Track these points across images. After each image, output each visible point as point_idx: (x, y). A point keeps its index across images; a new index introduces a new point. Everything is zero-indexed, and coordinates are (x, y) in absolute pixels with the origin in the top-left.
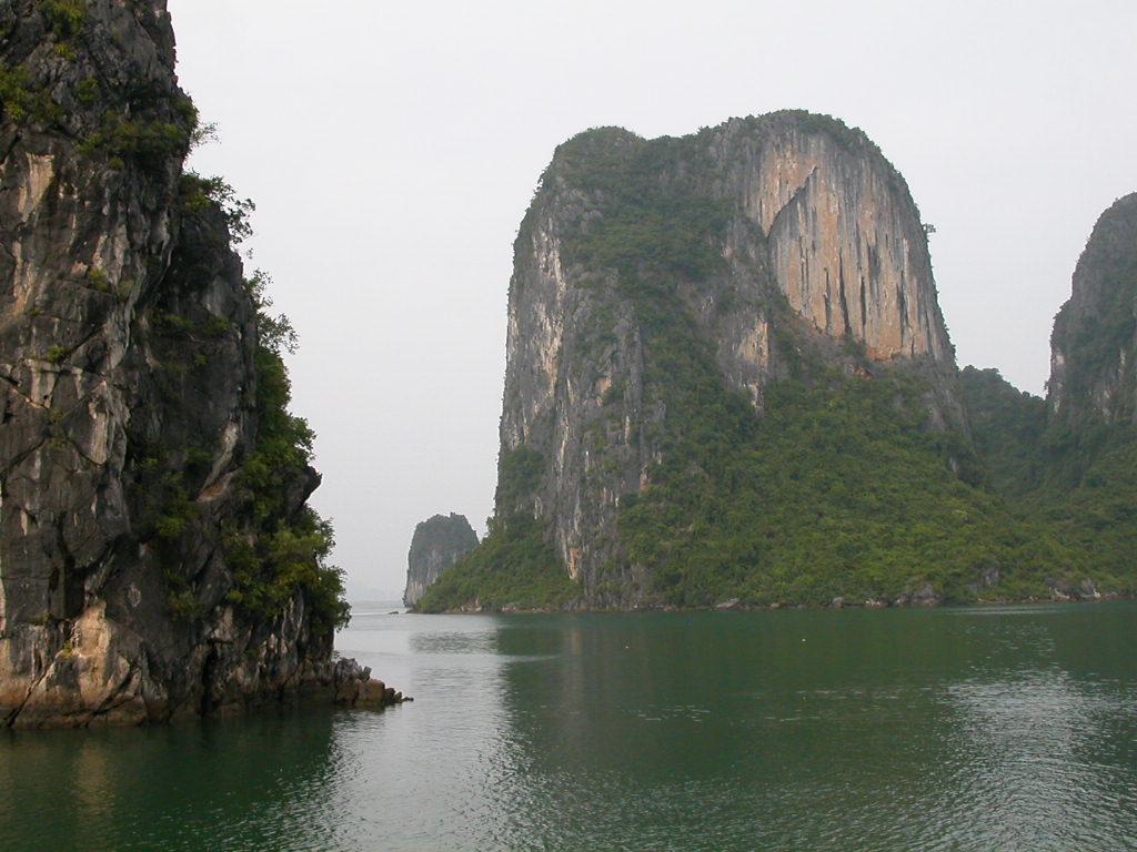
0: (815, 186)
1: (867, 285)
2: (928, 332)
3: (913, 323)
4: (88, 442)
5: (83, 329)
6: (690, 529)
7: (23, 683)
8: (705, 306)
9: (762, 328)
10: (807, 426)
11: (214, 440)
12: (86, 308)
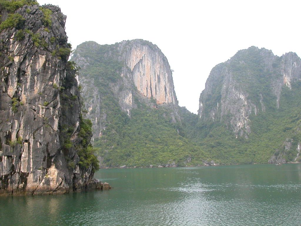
0: (144, 59)
1: (157, 85)
2: (172, 97)
3: (168, 95)
4: (53, 125)
5: (53, 98)
6: (113, 147)
7: (35, 184)
8: (116, 89)
9: (130, 95)
10: (142, 121)
11: (74, 125)
12: (54, 93)
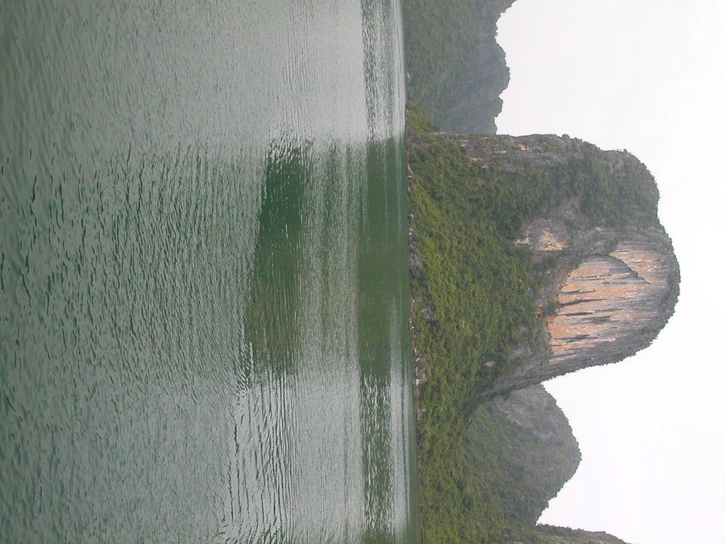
1: (588, 316)
3: (569, 345)
8: (568, 210)
9: (559, 247)
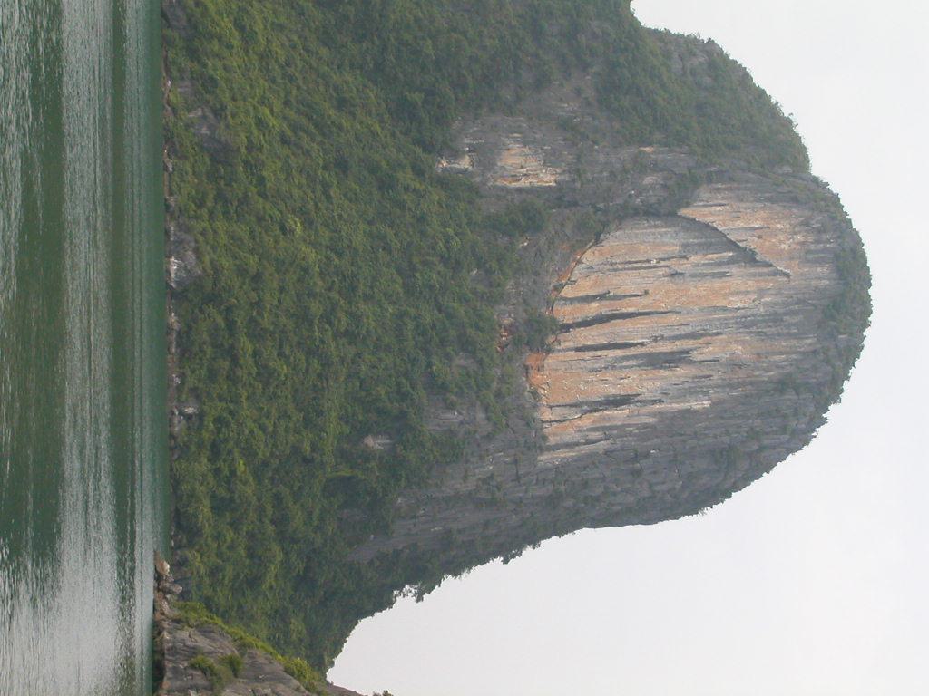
0: (761, 275)
1: (633, 351)
2: (577, 444)
3: (588, 421)
8: (564, 99)
9: (548, 179)
